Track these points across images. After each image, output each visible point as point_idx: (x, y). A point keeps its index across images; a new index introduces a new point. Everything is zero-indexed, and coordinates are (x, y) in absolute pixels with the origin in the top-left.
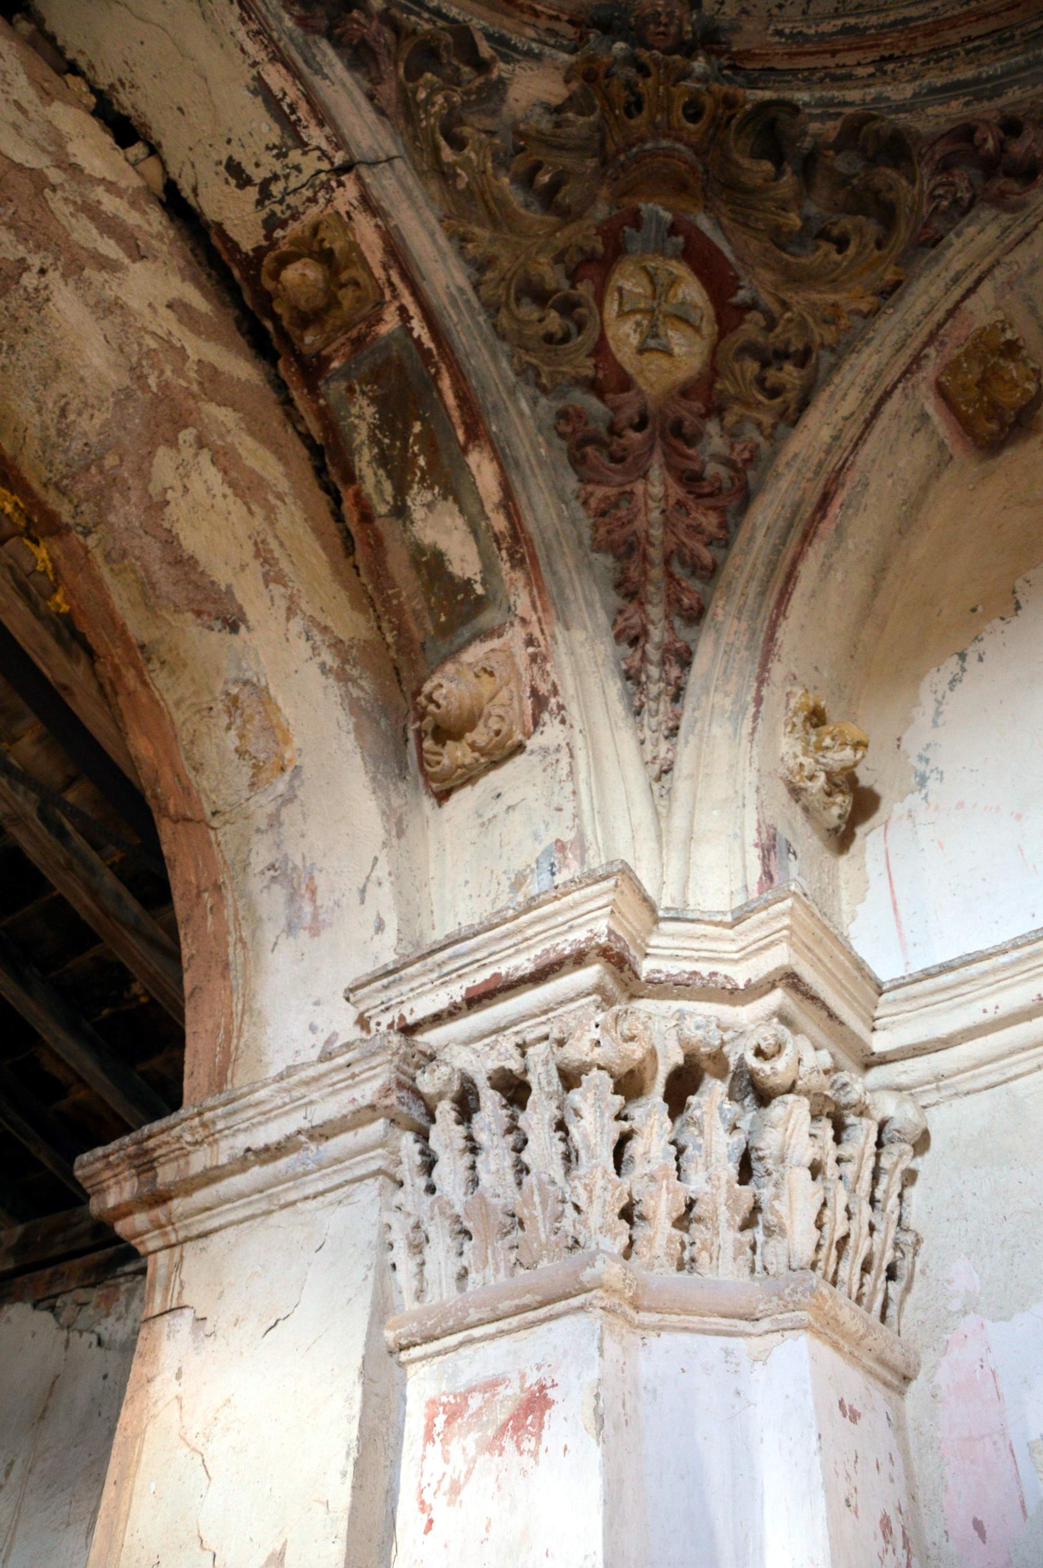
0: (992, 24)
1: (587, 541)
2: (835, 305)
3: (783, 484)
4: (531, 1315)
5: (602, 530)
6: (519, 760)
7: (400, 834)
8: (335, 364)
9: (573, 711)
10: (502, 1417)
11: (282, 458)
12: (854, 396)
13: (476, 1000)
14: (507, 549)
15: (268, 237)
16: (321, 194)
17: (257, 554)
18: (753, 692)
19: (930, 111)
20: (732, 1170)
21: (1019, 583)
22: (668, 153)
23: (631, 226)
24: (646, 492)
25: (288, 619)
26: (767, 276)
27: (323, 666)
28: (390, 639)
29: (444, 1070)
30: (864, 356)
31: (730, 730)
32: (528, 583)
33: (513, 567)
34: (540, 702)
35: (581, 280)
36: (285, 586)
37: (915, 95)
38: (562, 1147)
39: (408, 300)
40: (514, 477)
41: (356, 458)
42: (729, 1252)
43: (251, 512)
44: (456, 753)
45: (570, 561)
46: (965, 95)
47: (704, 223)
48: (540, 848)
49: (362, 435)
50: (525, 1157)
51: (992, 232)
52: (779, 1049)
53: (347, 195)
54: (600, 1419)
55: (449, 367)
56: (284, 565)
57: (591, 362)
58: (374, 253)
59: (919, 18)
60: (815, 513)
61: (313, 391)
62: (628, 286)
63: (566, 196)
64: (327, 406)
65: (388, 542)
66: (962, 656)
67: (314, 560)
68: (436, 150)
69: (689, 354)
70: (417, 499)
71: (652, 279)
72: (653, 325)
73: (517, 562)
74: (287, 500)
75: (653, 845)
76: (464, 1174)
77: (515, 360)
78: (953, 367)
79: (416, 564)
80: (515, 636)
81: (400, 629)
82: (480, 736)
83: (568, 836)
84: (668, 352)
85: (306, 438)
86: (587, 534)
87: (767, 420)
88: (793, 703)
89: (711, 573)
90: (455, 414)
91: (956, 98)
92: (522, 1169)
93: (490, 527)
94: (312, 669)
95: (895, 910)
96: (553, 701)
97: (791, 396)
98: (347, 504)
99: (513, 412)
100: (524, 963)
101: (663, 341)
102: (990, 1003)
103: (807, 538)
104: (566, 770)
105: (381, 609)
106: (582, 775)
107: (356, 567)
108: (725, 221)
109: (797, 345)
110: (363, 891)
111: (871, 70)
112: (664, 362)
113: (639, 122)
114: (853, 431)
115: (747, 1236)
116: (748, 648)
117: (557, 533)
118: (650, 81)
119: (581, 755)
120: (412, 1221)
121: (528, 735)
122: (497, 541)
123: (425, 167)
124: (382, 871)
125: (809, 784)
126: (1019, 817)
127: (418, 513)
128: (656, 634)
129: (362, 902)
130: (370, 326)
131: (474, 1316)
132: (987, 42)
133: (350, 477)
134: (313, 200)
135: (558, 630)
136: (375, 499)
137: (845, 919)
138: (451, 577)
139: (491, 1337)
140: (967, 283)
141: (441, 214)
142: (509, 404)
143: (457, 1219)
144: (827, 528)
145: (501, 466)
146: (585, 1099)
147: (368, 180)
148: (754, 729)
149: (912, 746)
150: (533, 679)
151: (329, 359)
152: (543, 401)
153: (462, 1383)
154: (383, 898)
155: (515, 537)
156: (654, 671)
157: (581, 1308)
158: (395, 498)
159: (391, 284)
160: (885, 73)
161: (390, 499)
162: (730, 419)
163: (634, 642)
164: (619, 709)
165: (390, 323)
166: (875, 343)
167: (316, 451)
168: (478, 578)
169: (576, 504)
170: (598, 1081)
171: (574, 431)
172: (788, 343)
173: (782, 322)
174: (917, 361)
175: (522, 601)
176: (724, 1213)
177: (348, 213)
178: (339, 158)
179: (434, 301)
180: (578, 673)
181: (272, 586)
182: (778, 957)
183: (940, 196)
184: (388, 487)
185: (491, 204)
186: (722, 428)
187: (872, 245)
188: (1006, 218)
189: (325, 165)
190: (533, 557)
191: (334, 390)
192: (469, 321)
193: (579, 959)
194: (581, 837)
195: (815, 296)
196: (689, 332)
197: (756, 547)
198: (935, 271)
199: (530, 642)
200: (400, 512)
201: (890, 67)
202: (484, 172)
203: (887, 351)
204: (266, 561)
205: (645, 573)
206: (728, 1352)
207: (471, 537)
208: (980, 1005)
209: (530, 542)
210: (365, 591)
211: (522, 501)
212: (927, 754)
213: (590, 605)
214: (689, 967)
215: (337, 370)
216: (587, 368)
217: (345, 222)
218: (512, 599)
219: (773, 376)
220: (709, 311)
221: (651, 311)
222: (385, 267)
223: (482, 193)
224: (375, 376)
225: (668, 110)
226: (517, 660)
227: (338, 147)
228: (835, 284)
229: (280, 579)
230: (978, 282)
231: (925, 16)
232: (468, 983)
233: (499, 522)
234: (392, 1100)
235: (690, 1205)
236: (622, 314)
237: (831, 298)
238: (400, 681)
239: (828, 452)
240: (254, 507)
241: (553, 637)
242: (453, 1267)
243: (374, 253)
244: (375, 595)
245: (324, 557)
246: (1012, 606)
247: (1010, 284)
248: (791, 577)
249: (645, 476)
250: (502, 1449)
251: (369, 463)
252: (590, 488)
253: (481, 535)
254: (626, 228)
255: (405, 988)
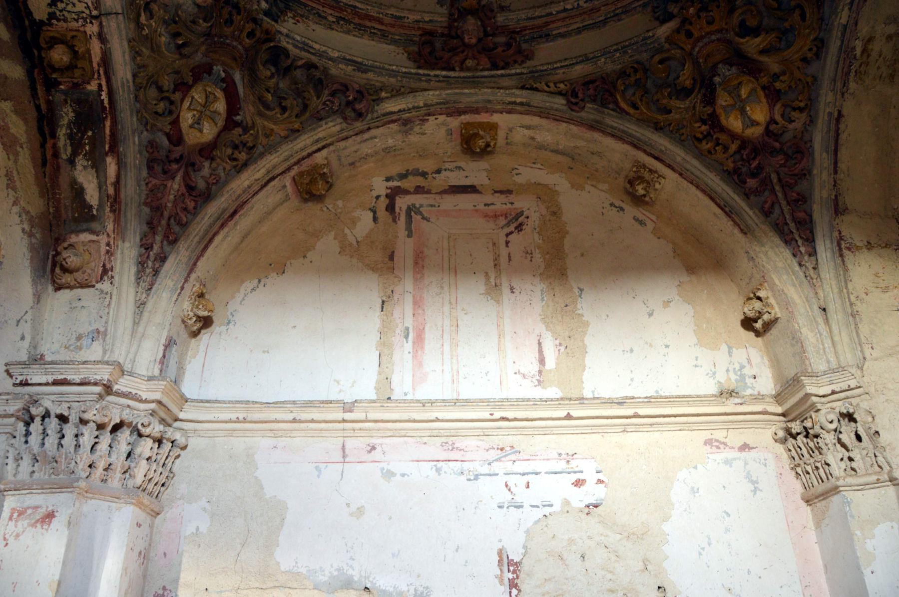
0: (383, 28)
1: (142, 201)
2: (272, 130)
3: (223, 199)
4: (54, 490)
5: (149, 200)
6: (92, 289)
7: (38, 302)
8: (62, 87)
9: (116, 278)
10: (38, 517)
11: (25, 121)
12: (263, 171)
13: (56, 383)
14: (111, 203)
15: (49, 19)
16: (81, 21)
17: (7, 175)
18: (181, 284)
19: (340, 66)
20: (125, 455)
21: (288, 263)
22: (234, 47)
23: (207, 73)
24: (172, 185)
25: (13, 205)
26: (252, 109)
27: (23, 230)
28: (51, 210)
29: (41, 409)
30: (273, 157)
31: (169, 296)
32: (114, 221)
33: (110, 211)
34: (105, 271)
35: (178, 91)
36: (16, 192)
37: (338, 57)
38: (75, 443)
39: (104, 83)
40: (122, 173)
41: (59, 129)
42: (117, 479)
43: (9, 158)
44: (67, 278)
45: (133, 212)
46: (355, 66)
47: (237, 77)
48: (91, 329)
49: (65, 121)
50: (63, 442)
51: (338, 128)
52: (149, 425)
53: (92, 29)
54: (69, 523)
55: (112, 119)
56: (18, 184)
57: (169, 127)
58: (96, 57)
59: (361, 9)
60: (229, 217)
61: (48, 92)
62: (196, 97)
63: (185, 51)
64: (53, 101)
65: (62, 171)
66: (260, 281)
67: (29, 177)
68: (139, 15)
69: (209, 134)
70: (80, 162)
71: (207, 97)
72: (199, 119)
73: (113, 211)
74: (24, 146)
75: (130, 337)
76: (39, 441)
77: (140, 115)
78: (301, 174)
79: (72, 187)
80: (103, 239)
81: (57, 210)
82: (79, 276)
83: (102, 329)
84: (201, 131)
85: (38, 107)
86: (144, 197)
87: (228, 167)
88: (195, 289)
89: (184, 226)
90: (108, 138)
91: (351, 65)
92: (60, 445)
93: (106, 190)
94: (18, 229)
95: (203, 366)
96: (110, 273)
97: (240, 163)
98: (48, 145)
99: (131, 141)
100: (77, 378)
101: (201, 127)
102: (217, 415)
103: (222, 226)
104: (107, 303)
105: (51, 196)
106: (112, 306)
107: (44, 173)
108: (245, 81)
109: (250, 144)
110: (18, 321)
111: (334, 20)
112: (198, 135)
113: (228, 30)
114: (256, 188)
115: (123, 476)
116: (186, 265)
117: (132, 199)
118: (239, 17)
119: (114, 297)
120: (17, 452)
121: (97, 282)
122: (108, 197)
123: (131, 17)
124: (28, 317)
125: (189, 321)
126: (251, 351)
127: (79, 167)
128: (156, 248)
129: (17, 325)
130: (84, 82)
131: (35, 487)
132: (379, 33)
133: (53, 135)
134: (77, 20)
135: (120, 243)
136: (62, 151)
137: (187, 362)
138: (85, 200)
139: (39, 494)
140: (320, 145)
141: (130, 36)
142: (131, 137)
143: (34, 455)
144: (231, 223)
145: (119, 167)
146: (86, 430)
147: (104, 24)
148: (177, 299)
149: (231, 307)
150: (105, 260)
151: (60, 83)
152: (145, 133)
153: (26, 505)
154: (26, 328)
155: (115, 200)
156: (150, 263)
157: (71, 492)
158: (71, 155)
159: (99, 73)
160: (339, 23)
161: (69, 154)
162: (214, 165)
163: (146, 249)
164: (133, 278)
165: (92, 87)
166: (278, 154)
167: (41, 118)
168: (96, 207)
169: (143, 183)
170: (92, 425)
171: (153, 152)
172: (247, 142)
173: (248, 134)
174: (289, 169)
175: (110, 227)
176: (119, 469)
177: (90, 35)
178: (95, 13)
179: (115, 86)
180: (122, 262)
181: (9, 190)
182: (157, 396)
183: (327, 105)
184: (69, 149)
185: (154, 45)
186: (210, 166)
187: (294, 116)
188: (344, 125)
189: (87, 12)
190: (120, 210)
191: (58, 97)
192: (126, 96)
193: (95, 384)
194: (106, 330)
195: (266, 123)
196: (213, 124)
197: (203, 222)
198: (312, 134)
199: (108, 244)
200: (72, 162)
201: (342, 22)
202: (156, 31)
203: (282, 158)
204: (10, 179)
205: (160, 222)
206: (109, 507)
207: (98, 190)
208: (214, 415)
209: (120, 203)
210: (46, 186)
211: (122, 183)
212: (234, 313)
213: (135, 233)
214: (130, 390)
215: (62, 90)
216: (167, 129)
217: (87, 38)
218: (106, 224)
219: (237, 155)
220: (224, 115)
221: (202, 112)
222: (99, 65)
223: (152, 40)
224: (79, 102)
225: (242, 31)
226: (101, 249)
227: (96, 9)
228: (275, 123)
229: (14, 189)
230: (324, 147)
231: (363, 9)
232: (55, 377)
233: (111, 191)
234: (20, 413)
235: (110, 465)
236: (189, 109)
237: (273, 126)
238: (51, 231)
239: (244, 192)
240: (11, 157)
241: (117, 246)
242: (31, 469)
243: (96, 57)
244: (49, 189)
245: (33, 172)
246: (282, 271)
247: (334, 151)
248: (211, 241)
249: (173, 179)
250: (36, 527)
251: (64, 135)
252: (150, 179)
253: (103, 190)
254: (205, 74)
255: (30, 370)
